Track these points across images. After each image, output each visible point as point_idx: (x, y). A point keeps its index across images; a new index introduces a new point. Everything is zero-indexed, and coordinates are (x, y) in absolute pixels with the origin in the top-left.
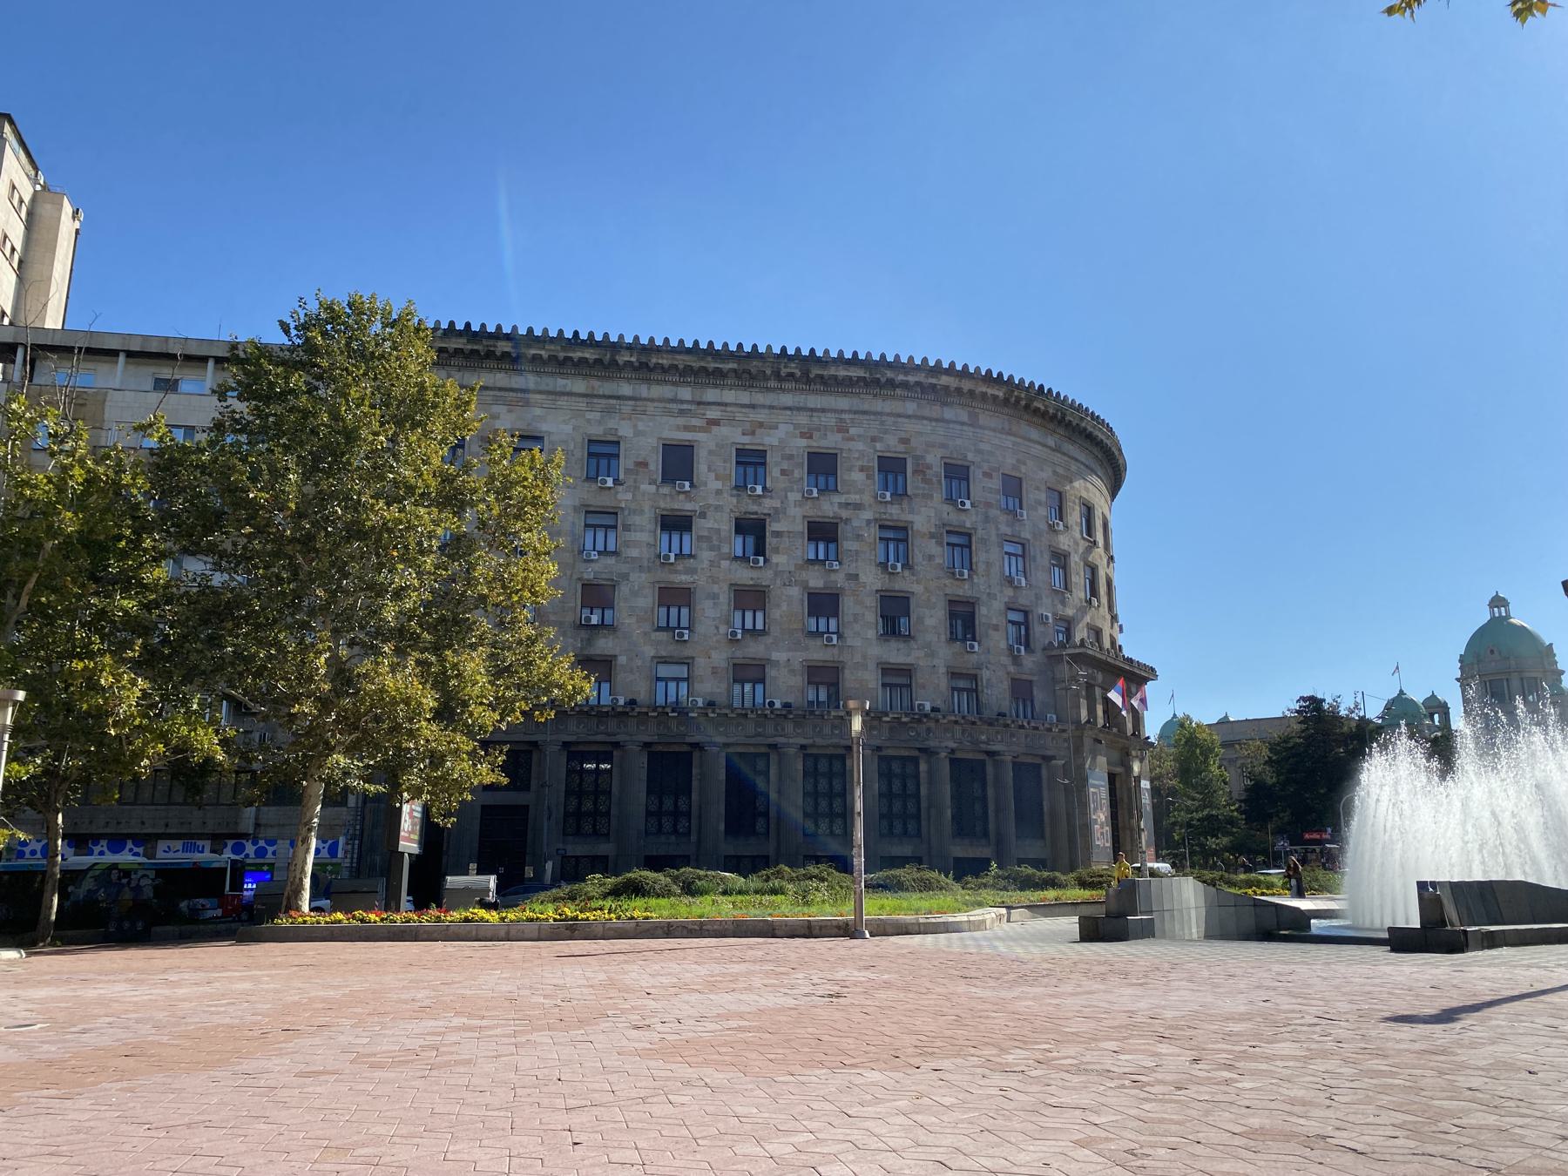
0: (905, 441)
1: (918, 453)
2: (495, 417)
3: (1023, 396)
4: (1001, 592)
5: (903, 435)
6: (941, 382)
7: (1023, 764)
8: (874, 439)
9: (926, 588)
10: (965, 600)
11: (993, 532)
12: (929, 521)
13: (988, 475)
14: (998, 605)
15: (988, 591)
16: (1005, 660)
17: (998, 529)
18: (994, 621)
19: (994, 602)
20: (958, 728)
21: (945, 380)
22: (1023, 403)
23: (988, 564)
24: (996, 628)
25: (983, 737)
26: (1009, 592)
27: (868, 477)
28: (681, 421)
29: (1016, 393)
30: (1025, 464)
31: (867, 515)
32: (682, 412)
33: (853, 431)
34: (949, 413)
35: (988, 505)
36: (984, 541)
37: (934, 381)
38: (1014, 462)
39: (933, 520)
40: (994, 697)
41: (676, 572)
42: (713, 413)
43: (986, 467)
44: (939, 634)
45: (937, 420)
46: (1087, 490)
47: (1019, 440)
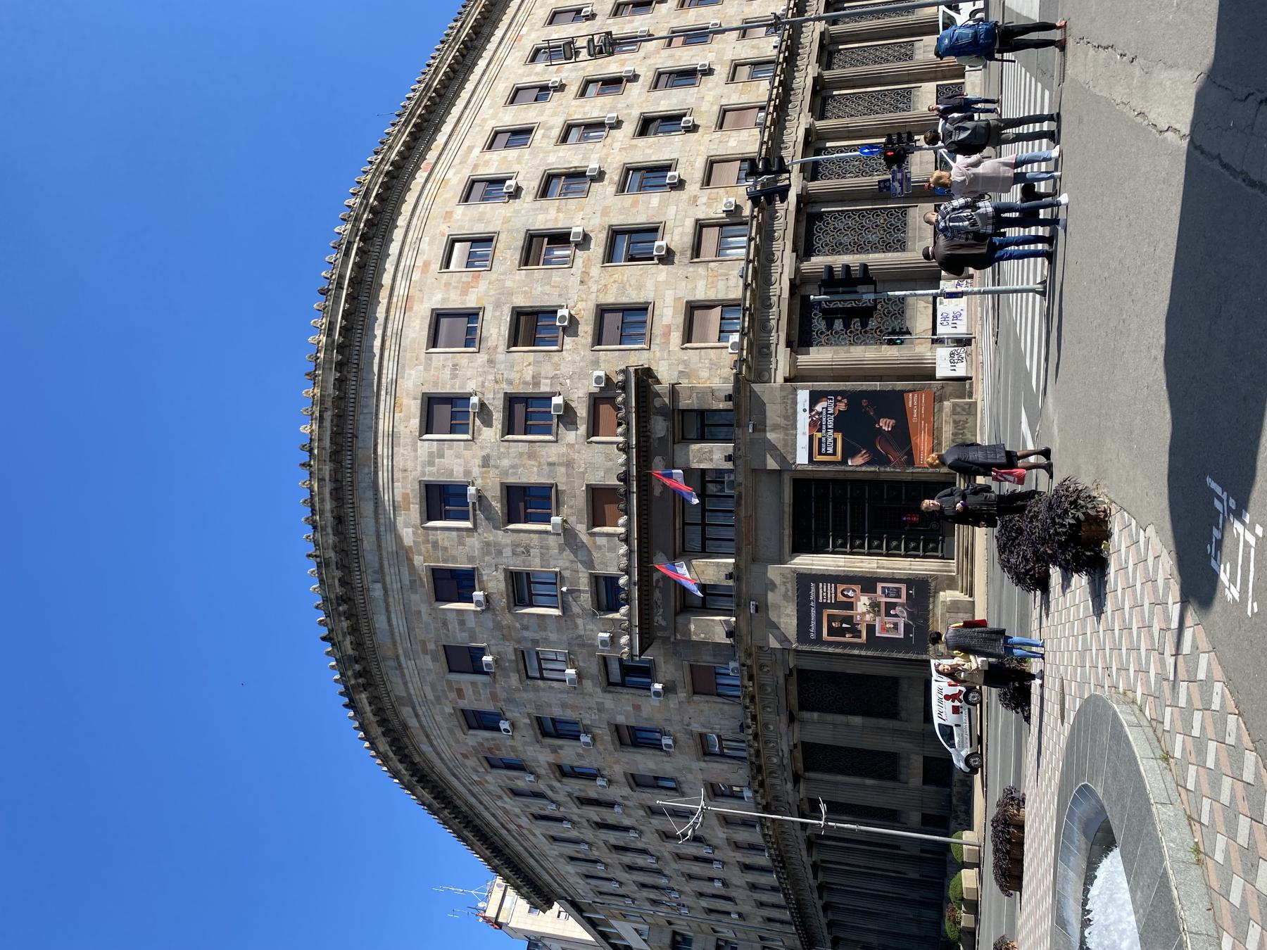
0: (465, 756)
1: (471, 749)
2: (578, 883)
3: (350, 673)
4: (591, 695)
5: (459, 756)
6: (388, 748)
7: (799, 694)
8: (477, 771)
9: (617, 762)
10: (615, 734)
11: (525, 695)
12: (541, 752)
13: (460, 693)
14: (608, 701)
15: (596, 711)
16: (673, 702)
17: (517, 690)
18: (630, 708)
19: (606, 706)
20: (768, 781)
21: (383, 745)
22: (357, 667)
23: (564, 706)
24: (637, 708)
25: (775, 760)
26: (588, 684)
27: (518, 779)
28: (531, 837)
29: (353, 682)
30: (423, 643)
31: (556, 784)
32: (522, 835)
33: (476, 778)
34: (413, 722)
35: (494, 697)
36: (538, 707)
37: (391, 754)
38: (428, 658)
39: (540, 749)
40: (722, 722)
41: (663, 856)
42: (513, 827)
43: (453, 695)
44: (663, 761)
45: (427, 736)
46: (406, 496)
47: (400, 652)
